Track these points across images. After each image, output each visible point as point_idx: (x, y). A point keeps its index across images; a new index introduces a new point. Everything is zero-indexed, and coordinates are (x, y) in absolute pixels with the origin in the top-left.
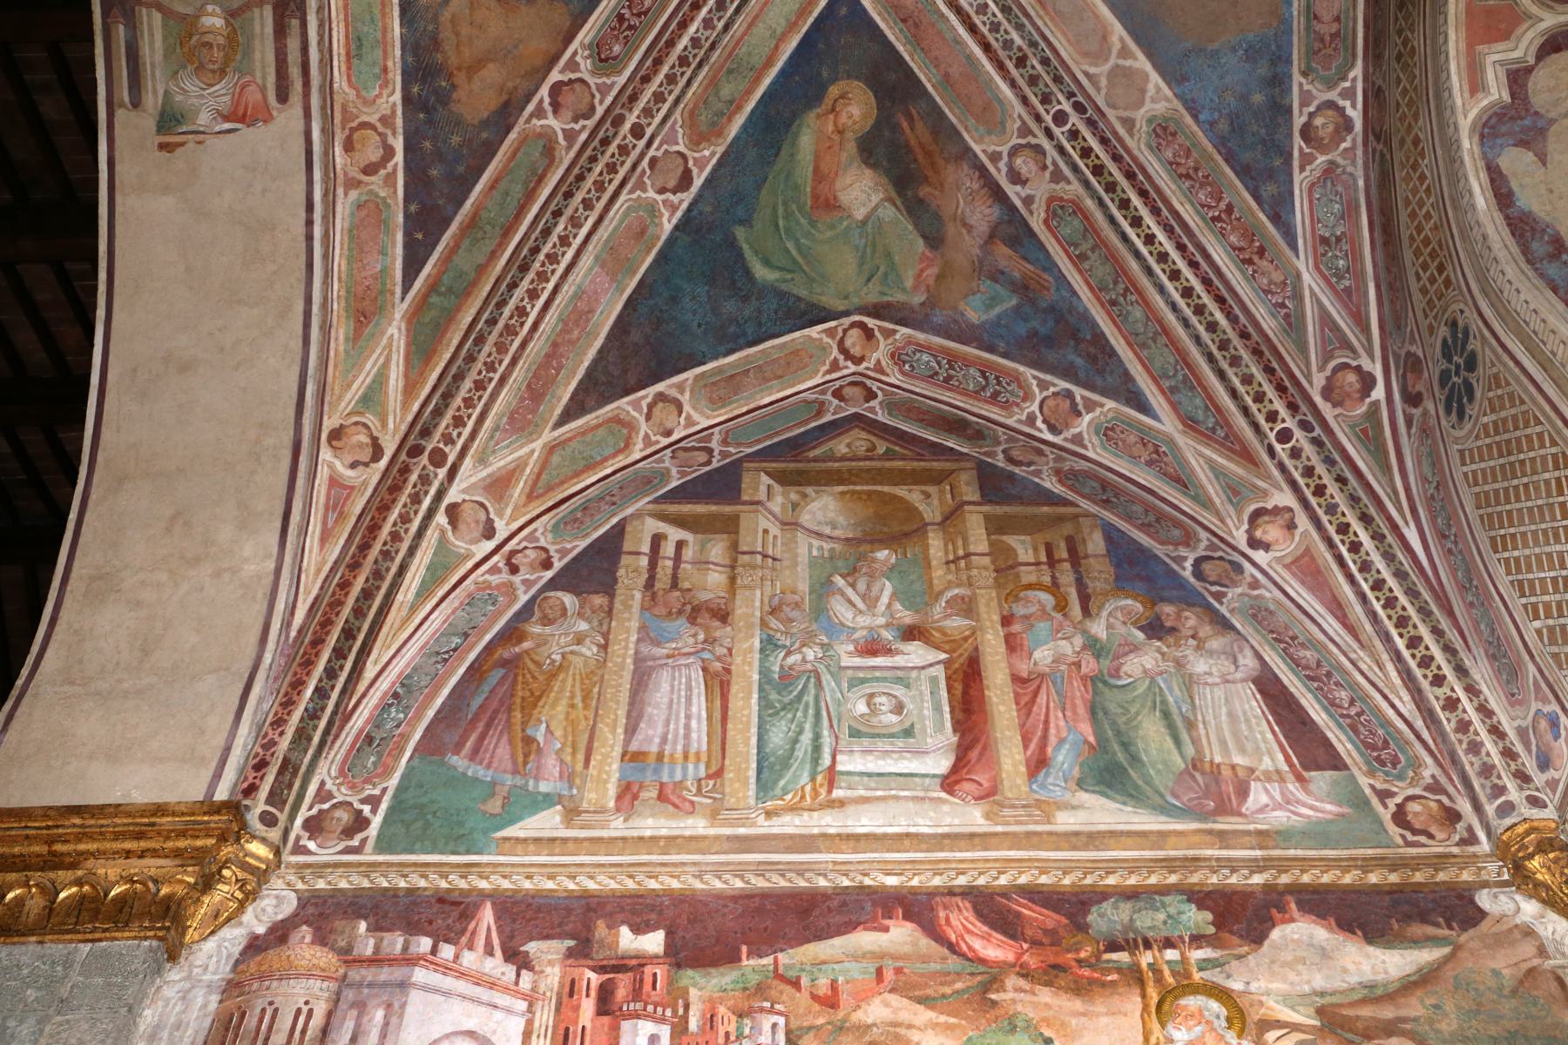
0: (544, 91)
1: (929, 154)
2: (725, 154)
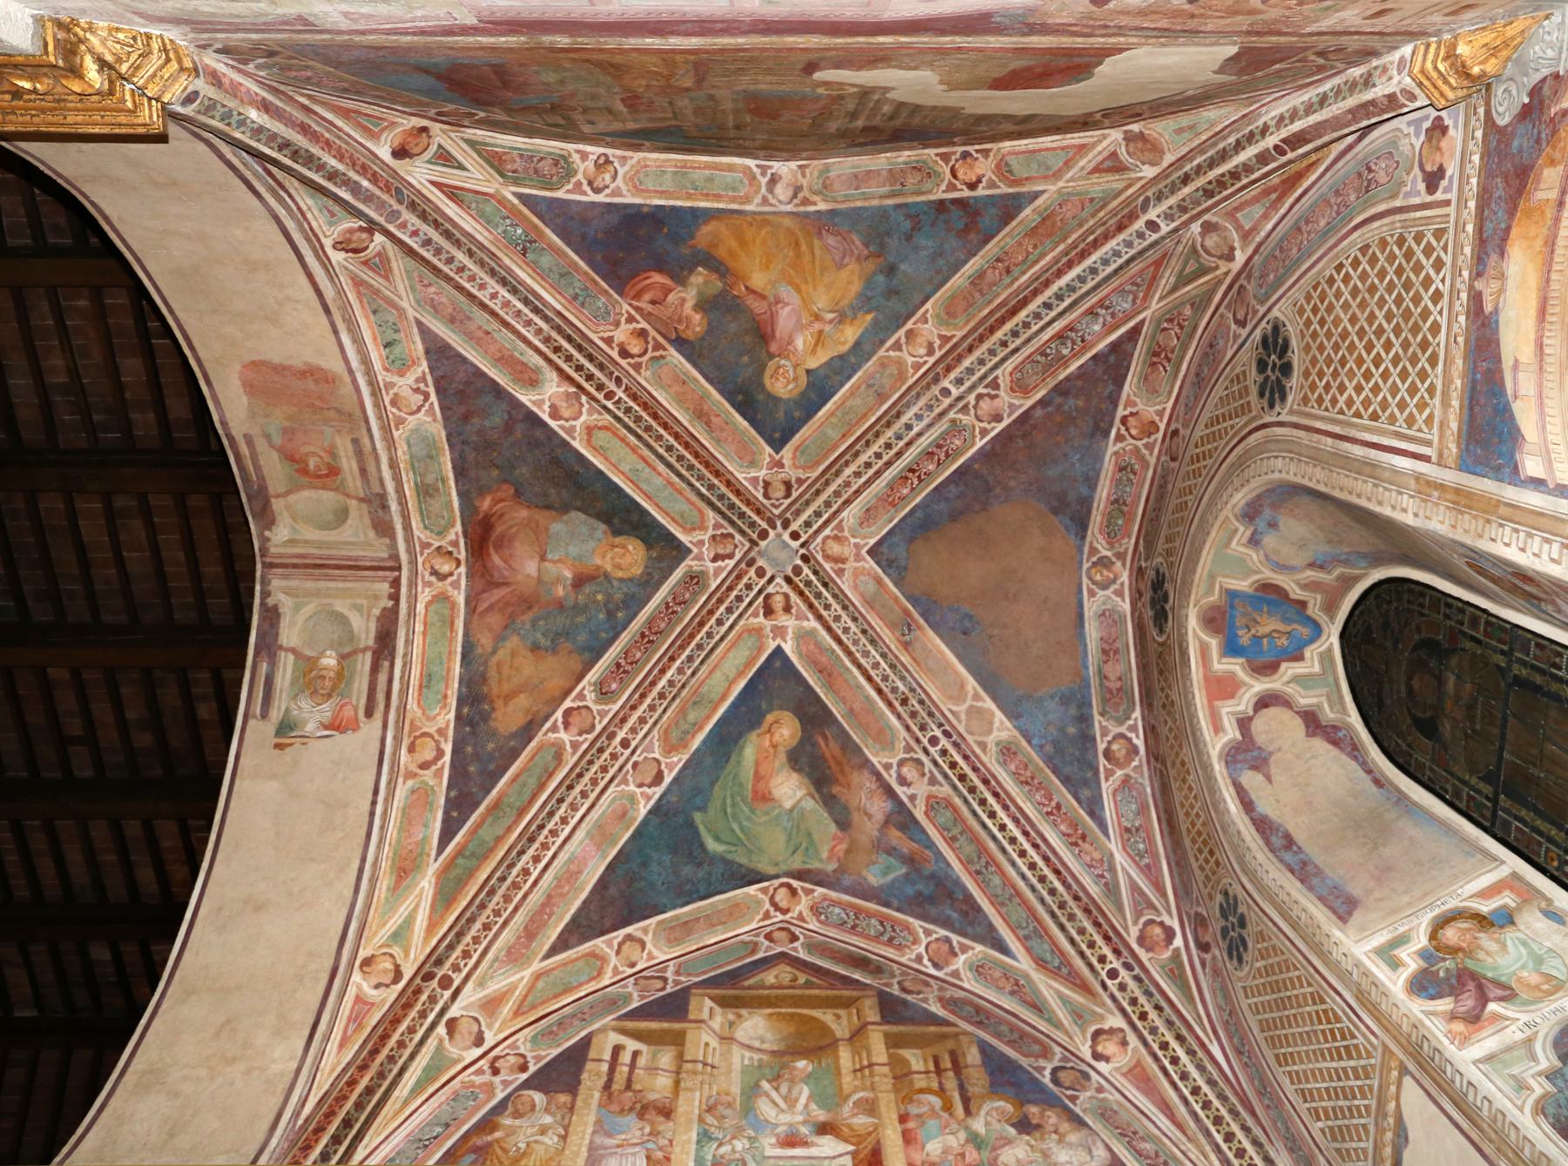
0: (559, 714)
1: (839, 763)
2: (689, 761)
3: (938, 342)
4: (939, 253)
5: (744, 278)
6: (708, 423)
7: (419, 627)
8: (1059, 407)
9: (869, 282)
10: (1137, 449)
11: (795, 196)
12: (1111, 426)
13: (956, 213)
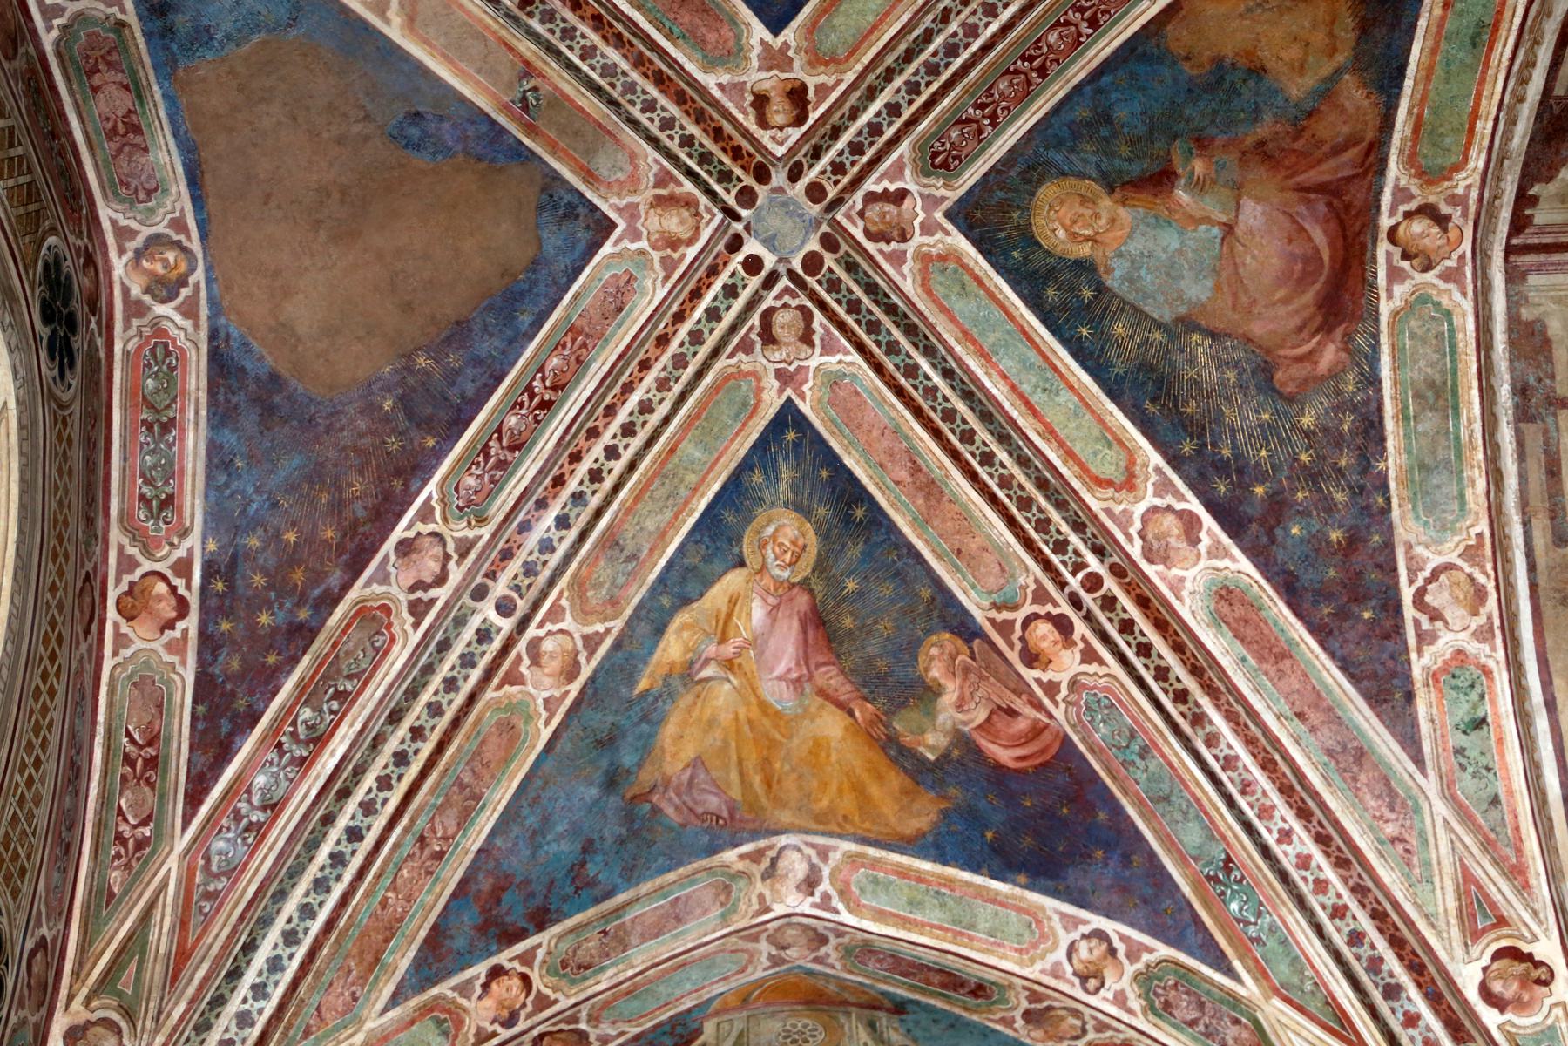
3: (523, 669)
4: (536, 837)
5: (854, 729)
6: (916, 469)
7: (1484, 127)
8: (301, 601)
9: (647, 747)
10: (149, 555)
11: (774, 861)
12: (204, 588)
13: (517, 918)
